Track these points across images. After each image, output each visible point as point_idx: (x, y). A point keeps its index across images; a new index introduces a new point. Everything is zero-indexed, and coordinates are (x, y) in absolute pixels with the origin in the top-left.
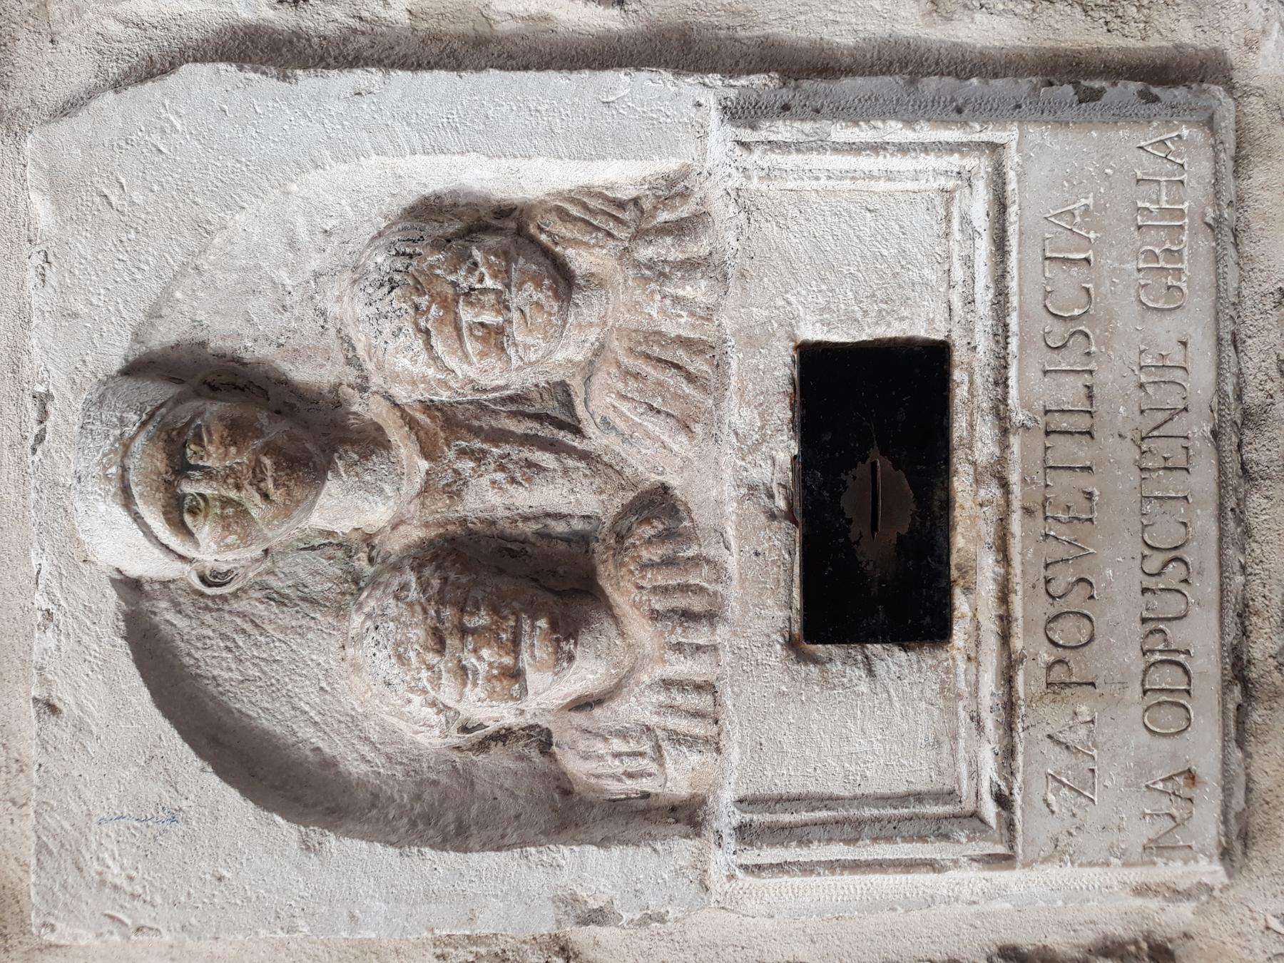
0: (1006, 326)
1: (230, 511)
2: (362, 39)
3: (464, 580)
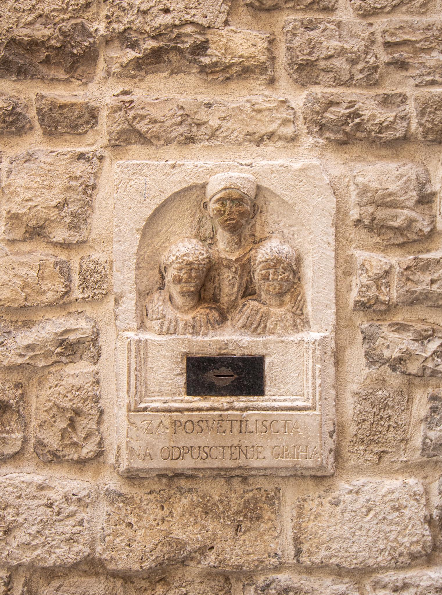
1: (222, 212)
3: (204, 269)
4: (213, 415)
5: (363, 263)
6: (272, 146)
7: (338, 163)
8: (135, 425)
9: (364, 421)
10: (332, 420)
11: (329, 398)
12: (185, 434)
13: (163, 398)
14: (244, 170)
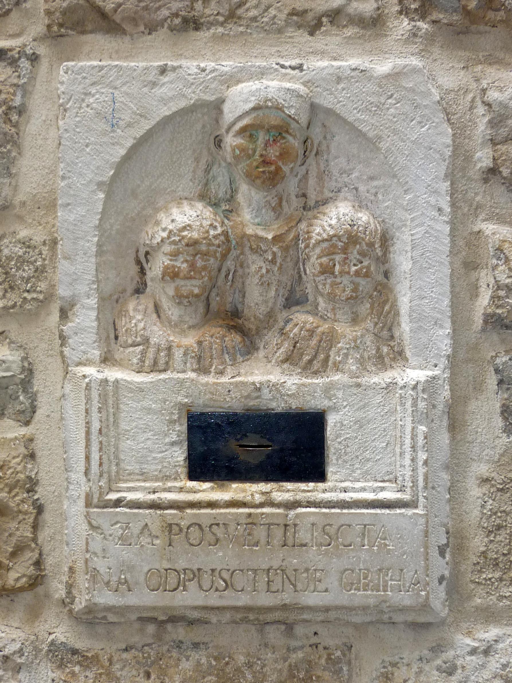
0: (334, 507)
2: (466, 209)
4: (236, 513)
5: (500, 246)
6: (337, 35)
7: (453, 67)
8: (100, 531)
9: (499, 527)
10: (445, 525)
11: (439, 486)
12: (187, 546)
13: (147, 485)
14: (288, 77)
